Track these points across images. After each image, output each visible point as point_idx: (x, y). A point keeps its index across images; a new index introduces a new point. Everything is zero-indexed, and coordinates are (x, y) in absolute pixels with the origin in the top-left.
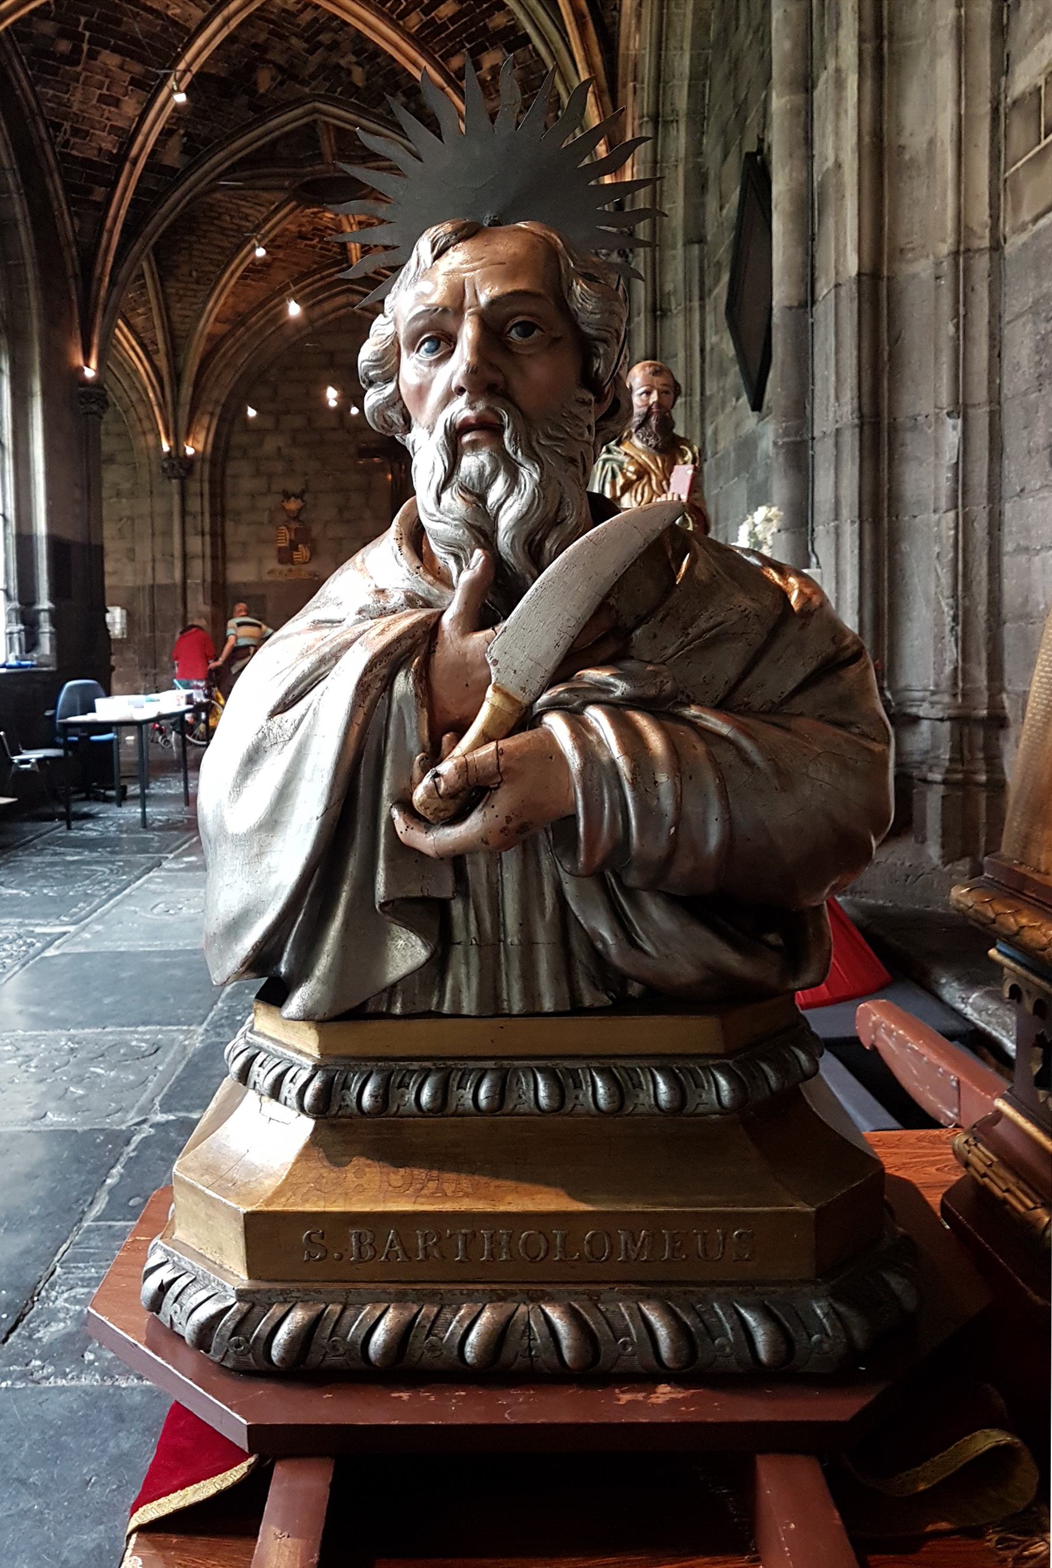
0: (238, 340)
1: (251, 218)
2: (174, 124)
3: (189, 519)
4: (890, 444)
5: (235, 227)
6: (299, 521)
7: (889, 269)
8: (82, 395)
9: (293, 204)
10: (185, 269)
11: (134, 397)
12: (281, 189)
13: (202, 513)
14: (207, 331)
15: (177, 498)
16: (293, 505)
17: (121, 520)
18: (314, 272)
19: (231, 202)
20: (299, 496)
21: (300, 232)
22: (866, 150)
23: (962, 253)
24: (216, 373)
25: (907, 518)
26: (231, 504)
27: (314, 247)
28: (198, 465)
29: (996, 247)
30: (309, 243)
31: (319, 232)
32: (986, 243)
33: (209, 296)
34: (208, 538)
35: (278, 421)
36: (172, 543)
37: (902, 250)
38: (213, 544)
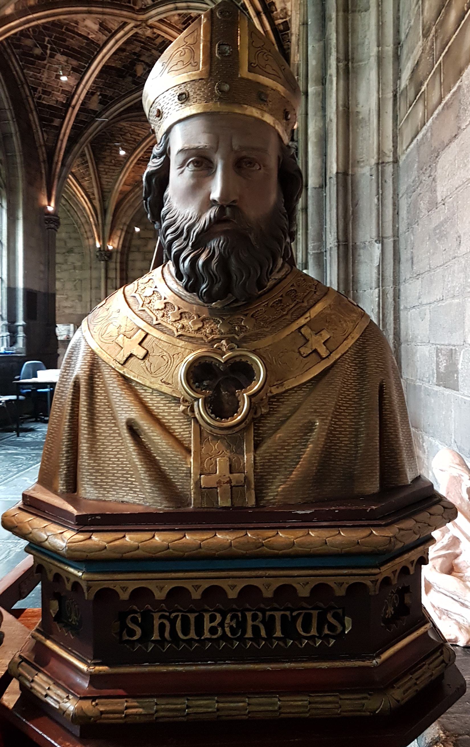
0: (136, 194)
1: (141, 135)
2: (94, 90)
3: (109, 281)
4: (353, 255)
5: (133, 139)
7: (352, 171)
8: (46, 219)
10: (108, 159)
11: (83, 220)
13: (116, 278)
14: (119, 189)
15: (103, 271)
17: (75, 281)
19: (130, 127)
22: (340, 114)
23: (380, 163)
25: (361, 292)
28: (114, 255)
29: (396, 161)
32: (391, 159)
33: (121, 172)
36: (100, 293)
37: (358, 162)
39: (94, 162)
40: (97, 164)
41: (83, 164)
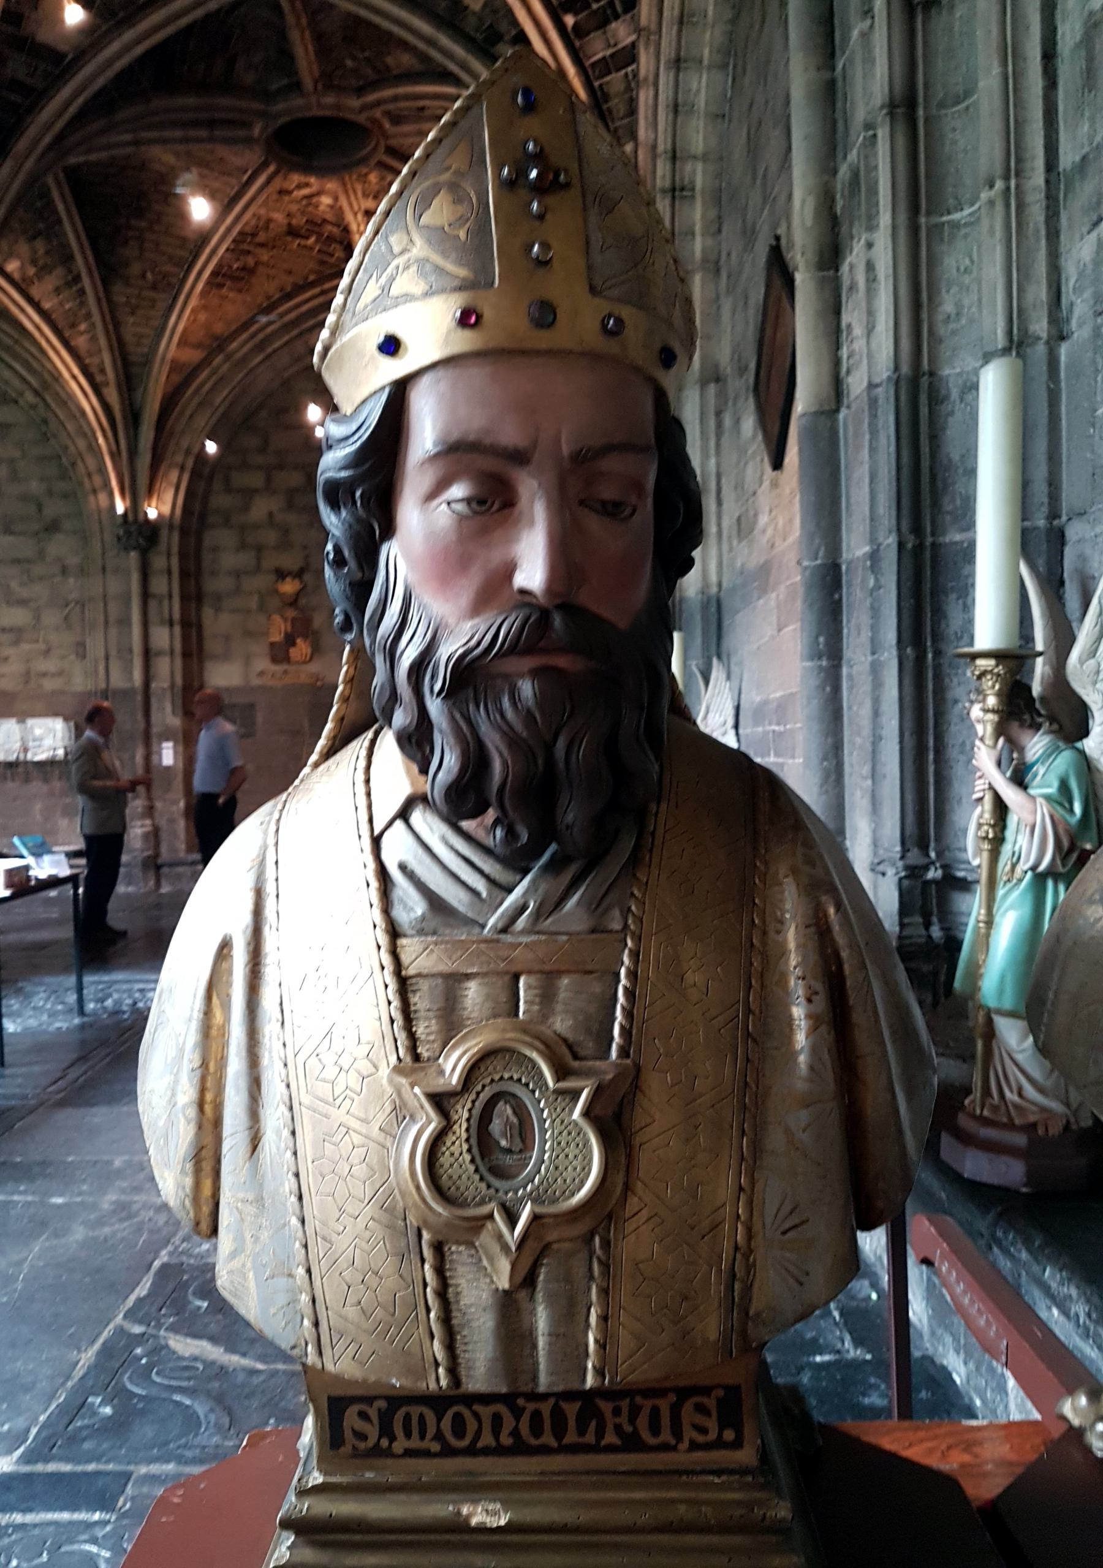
3: (153, 604)
6: (297, 608)
9: (272, 168)
10: (136, 268)
11: (81, 444)
12: (248, 141)
13: (170, 596)
15: (135, 578)
16: (289, 587)
17: (67, 605)
18: (313, 285)
20: (299, 574)
21: (289, 224)
24: (188, 413)
26: (212, 585)
27: (311, 248)
28: (164, 533)
30: (303, 242)
31: (315, 225)
34: (177, 629)
35: (269, 479)
36: (130, 633)
38: (185, 638)
39: (96, 274)
40: (106, 283)
41: (68, 284)
